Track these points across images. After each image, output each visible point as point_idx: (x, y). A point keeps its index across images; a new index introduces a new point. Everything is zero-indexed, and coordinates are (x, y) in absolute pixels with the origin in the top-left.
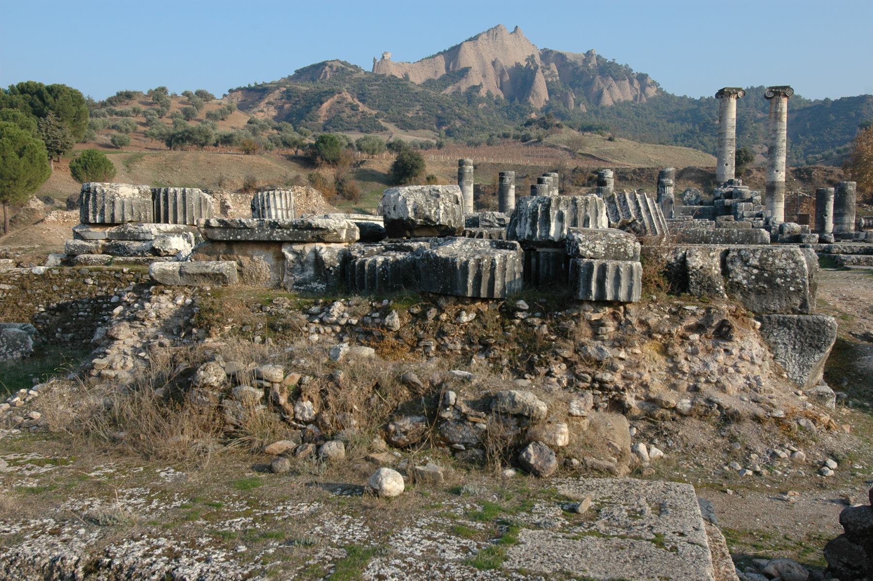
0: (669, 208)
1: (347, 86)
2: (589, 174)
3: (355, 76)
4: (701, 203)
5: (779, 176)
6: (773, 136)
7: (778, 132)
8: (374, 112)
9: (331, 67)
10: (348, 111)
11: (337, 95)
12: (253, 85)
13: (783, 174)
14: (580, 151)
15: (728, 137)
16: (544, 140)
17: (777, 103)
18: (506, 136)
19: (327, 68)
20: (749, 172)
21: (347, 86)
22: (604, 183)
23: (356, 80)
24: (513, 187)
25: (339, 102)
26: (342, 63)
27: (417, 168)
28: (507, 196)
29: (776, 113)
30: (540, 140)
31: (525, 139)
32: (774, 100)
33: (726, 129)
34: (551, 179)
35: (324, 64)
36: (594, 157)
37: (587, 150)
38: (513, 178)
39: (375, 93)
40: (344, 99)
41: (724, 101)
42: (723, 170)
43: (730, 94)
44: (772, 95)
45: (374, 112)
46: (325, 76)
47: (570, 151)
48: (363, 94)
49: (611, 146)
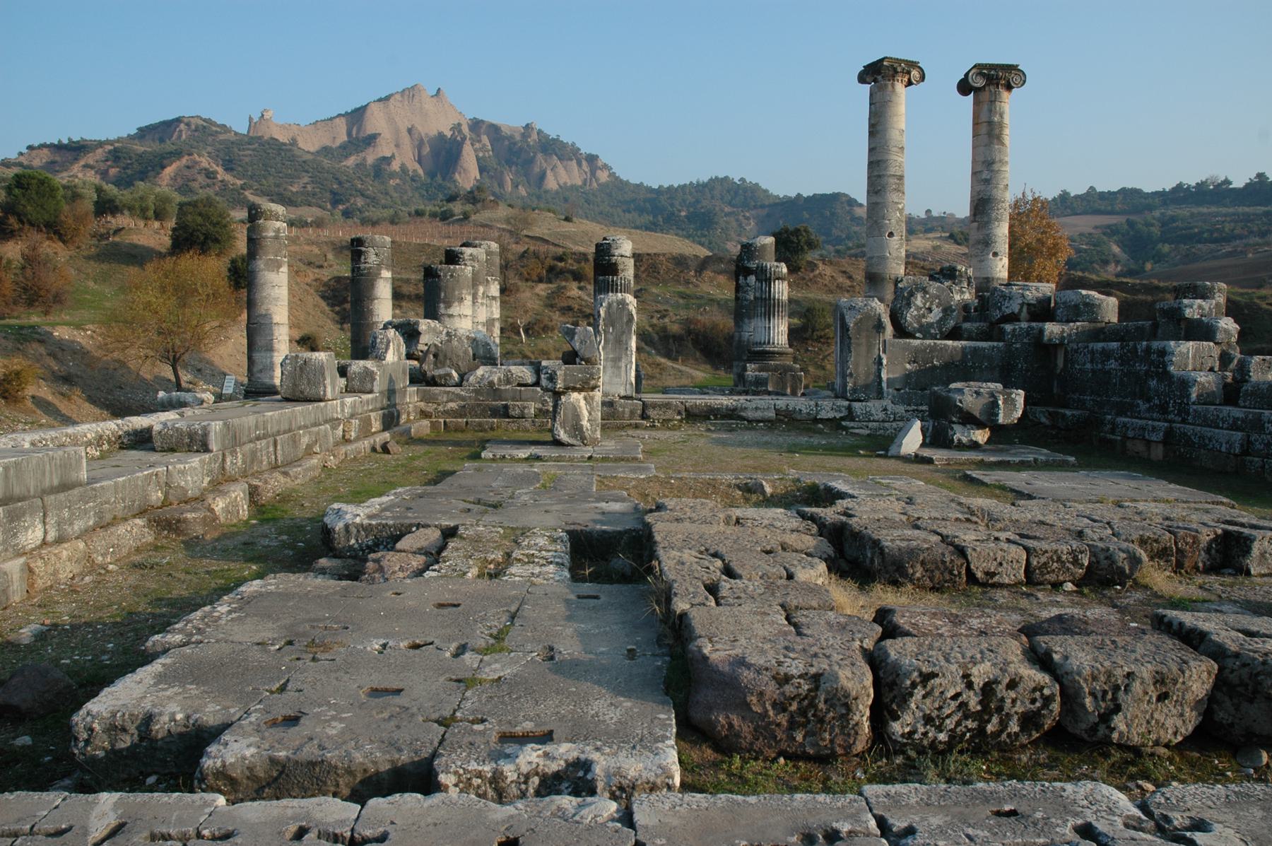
0: (870, 347)
1: (209, 149)
2: (549, 262)
3: (222, 137)
4: (954, 334)
5: (1000, 264)
6: (985, 175)
7: (996, 167)
8: (239, 182)
9: (188, 124)
10: (201, 179)
11: (186, 157)
12: (66, 141)
13: (1006, 261)
14: (525, 232)
15: (892, 171)
16: (473, 218)
17: (992, 102)
18: (419, 214)
19: (182, 126)
20: (812, 266)
21: (209, 149)
22: (612, 269)
23: (221, 142)
24: (387, 274)
25: (188, 167)
26: (204, 120)
27: (217, 241)
28: (371, 299)
29: (990, 123)
30: (466, 217)
31: (445, 217)
32: (985, 96)
33: (887, 151)
34: (480, 252)
35: (178, 120)
36: (546, 241)
37: (537, 231)
38: (386, 252)
39: (247, 159)
40: (196, 163)
41: (882, 88)
42: (882, 247)
43: (896, 72)
44: (980, 82)
45: (239, 182)
46: (180, 136)
47: (510, 232)
48: (230, 161)
49: (569, 228)
